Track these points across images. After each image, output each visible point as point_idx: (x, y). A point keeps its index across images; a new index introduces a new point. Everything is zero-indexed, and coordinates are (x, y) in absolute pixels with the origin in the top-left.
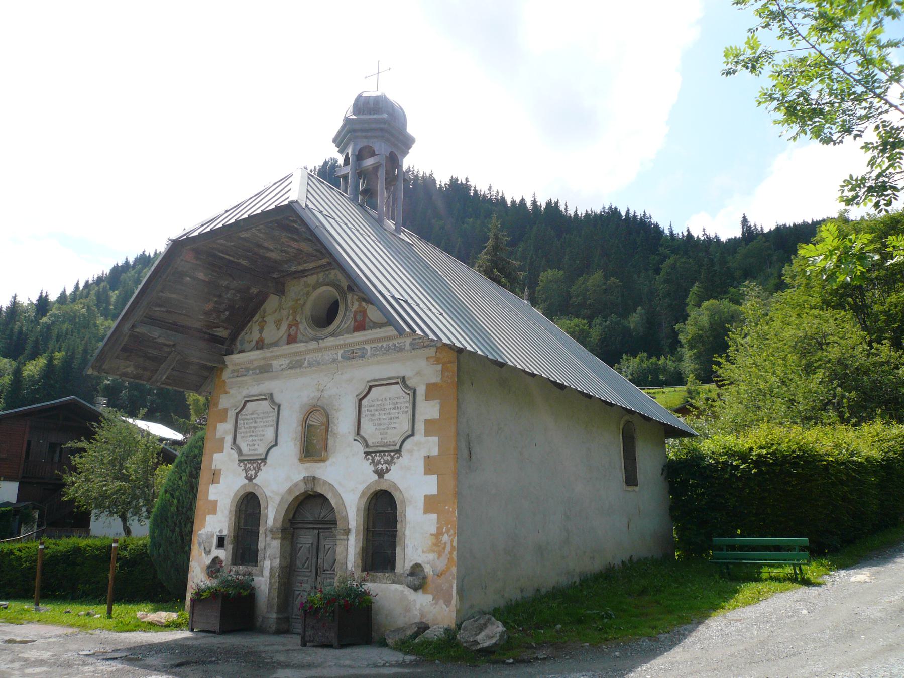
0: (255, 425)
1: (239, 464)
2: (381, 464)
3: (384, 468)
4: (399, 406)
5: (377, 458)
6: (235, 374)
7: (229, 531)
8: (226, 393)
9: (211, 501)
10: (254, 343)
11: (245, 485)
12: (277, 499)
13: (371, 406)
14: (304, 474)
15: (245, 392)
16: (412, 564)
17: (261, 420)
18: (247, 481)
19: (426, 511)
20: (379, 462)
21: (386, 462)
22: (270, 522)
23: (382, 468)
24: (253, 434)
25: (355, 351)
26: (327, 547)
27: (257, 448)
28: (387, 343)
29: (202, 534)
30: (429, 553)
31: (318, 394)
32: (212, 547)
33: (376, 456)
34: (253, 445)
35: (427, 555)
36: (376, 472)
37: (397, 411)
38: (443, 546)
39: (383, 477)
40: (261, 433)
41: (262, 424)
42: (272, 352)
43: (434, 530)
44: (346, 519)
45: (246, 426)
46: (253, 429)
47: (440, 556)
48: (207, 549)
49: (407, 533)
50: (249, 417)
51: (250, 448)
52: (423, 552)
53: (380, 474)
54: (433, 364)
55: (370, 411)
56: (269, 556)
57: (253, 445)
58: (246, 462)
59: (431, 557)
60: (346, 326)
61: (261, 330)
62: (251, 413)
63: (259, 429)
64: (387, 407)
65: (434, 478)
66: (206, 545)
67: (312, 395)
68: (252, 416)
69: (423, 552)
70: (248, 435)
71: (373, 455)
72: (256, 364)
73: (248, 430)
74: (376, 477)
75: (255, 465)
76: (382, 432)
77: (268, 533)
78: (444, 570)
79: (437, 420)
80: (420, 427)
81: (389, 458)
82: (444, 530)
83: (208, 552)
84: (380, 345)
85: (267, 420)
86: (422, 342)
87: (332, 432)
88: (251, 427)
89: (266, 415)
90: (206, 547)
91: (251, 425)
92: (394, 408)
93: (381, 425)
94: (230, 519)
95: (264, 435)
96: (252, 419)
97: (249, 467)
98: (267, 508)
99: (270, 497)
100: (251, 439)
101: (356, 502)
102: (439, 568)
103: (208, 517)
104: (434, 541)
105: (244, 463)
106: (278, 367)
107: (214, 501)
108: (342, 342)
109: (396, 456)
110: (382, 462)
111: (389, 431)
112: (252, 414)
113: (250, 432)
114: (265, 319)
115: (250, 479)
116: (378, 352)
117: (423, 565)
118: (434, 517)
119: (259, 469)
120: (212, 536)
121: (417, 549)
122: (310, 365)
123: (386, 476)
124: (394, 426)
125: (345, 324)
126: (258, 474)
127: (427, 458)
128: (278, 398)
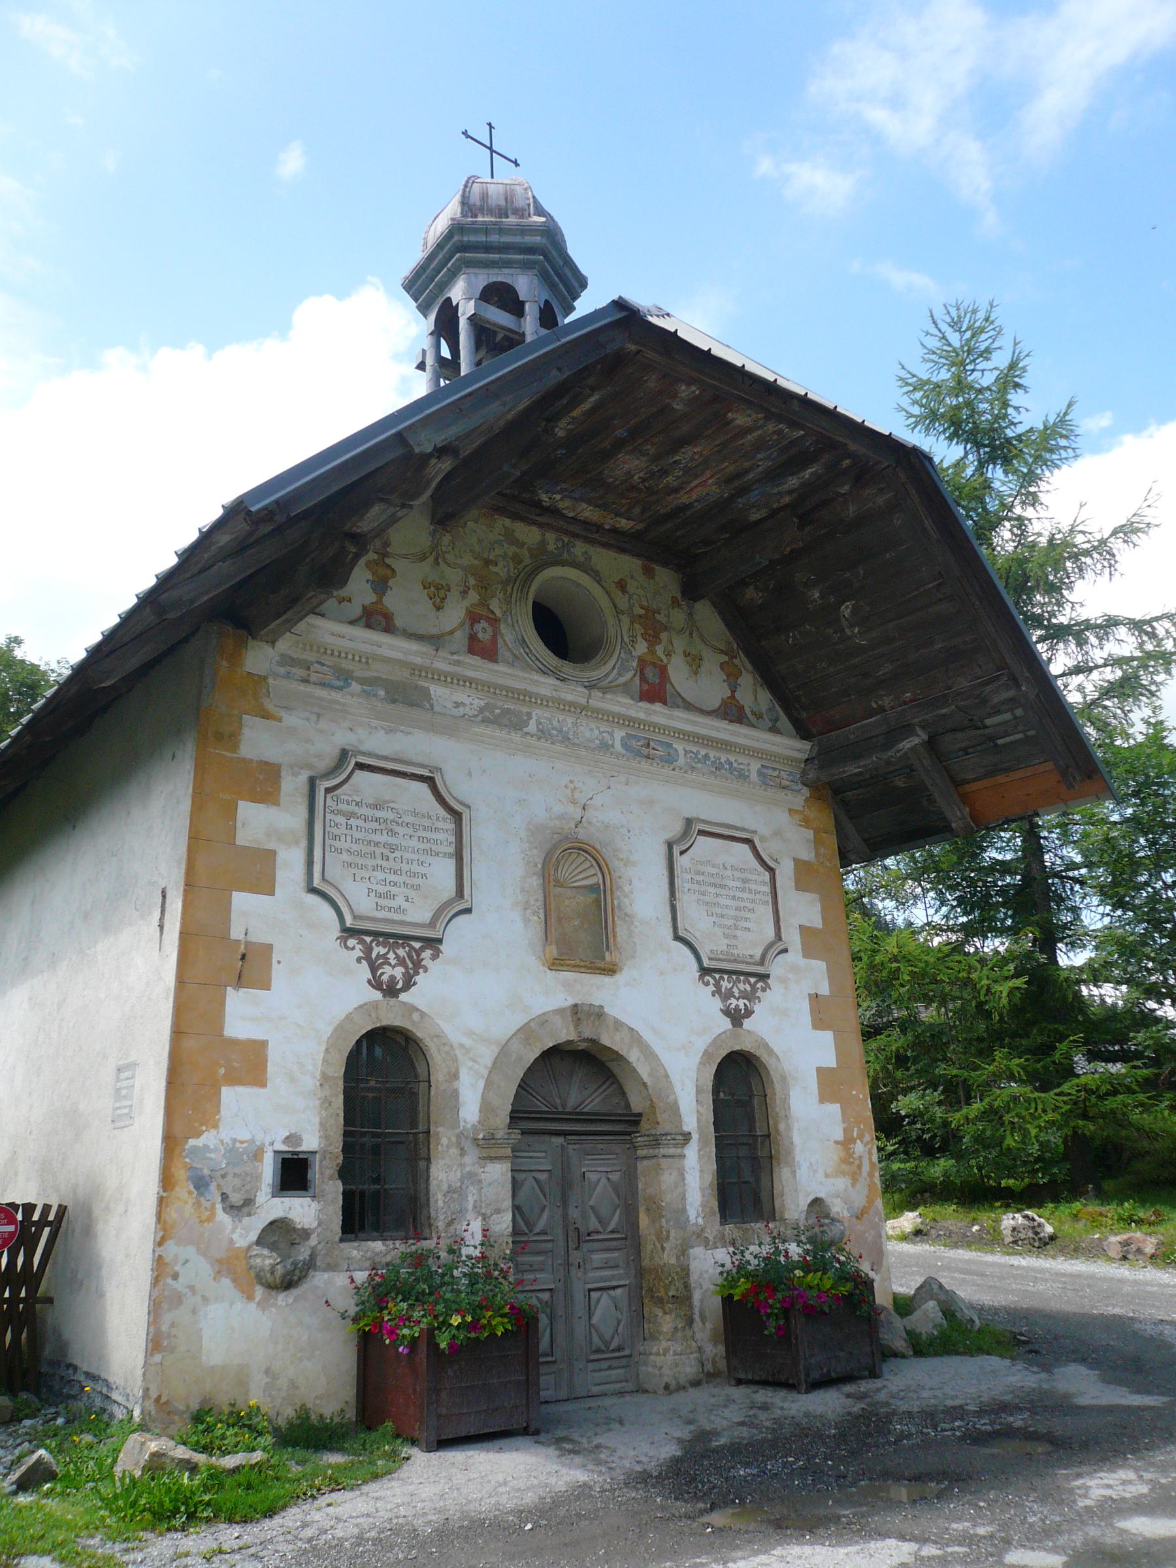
0: (391, 840)
1: (343, 940)
2: (735, 997)
3: (742, 1007)
4: (753, 887)
5: (725, 984)
6: (299, 672)
7: (326, 1137)
8: (267, 716)
9: (234, 1042)
10: (357, 611)
11: (375, 1005)
12: (487, 1055)
13: (698, 873)
14: (562, 1000)
15: (342, 738)
16: (809, 1200)
17: (410, 831)
18: (377, 995)
19: (823, 1099)
20: (729, 995)
21: (744, 995)
22: (470, 1111)
23: (737, 1006)
24: (385, 864)
25: (652, 744)
26: (593, 1177)
27: (405, 905)
28: (717, 754)
29: (206, 1146)
30: (836, 1176)
31: (576, 812)
32: (258, 1189)
33: (722, 978)
34: (387, 896)
35: (833, 1180)
36: (727, 1012)
37: (751, 896)
38: (857, 1163)
39: (741, 1025)
40: (415, 868)
41: (414, 843)
42: (457, 663)
43: (839, 1135)
44: (675, 1109)
45: (357, 835)
46: (386, 852)
47: (854, 1181)
48: (236, 1198)
49: (797, 1139)
50: (364, 811)
51: (381, 902)
52: (827, 1176)
53: (736, 1017)
54: (801, 825)
55: (698, 883)
56: (475, 1207)
57: (387, 896)
58: (368, 939)
59: (841, 1183)
60: (622, 680)
61: (381, 585)
62: (371, 801)
63: (407, 855)
64: (731, 883)
65: (828, 1036)
66: (229, 1185)
67: (558, 809)
68: (379, 814)
69: (827, 1176)
70: (371, 862)
71: (717, 976)
72: (378, 670)
73: (365, 849)
74: (726, 1024)
75: (401, 952)
76: (727, 931)
77: (468, 1145)
78: (864, 1206)
79: (820, 931)
80: (792, 938)
81: (748, 988)
82: (855, 1135)
83: (241, 1208)
84: (703, 752)
85: (435, 836)
86: (778, 777)
87: (619, 908)
88: (377, 844)
89: (427, 823)
90: (228, 1191)
91: (377, 838)
92: (744, 890)
93: (722, 916)
94: (326, 1102)
95: (424, 876)
96: (378, 820)
97: (384, 956)
98: (455, 1076)
99: (462, 1046)
100: (380, 875)
101: (694, 1075)
102: (857, 1204)
103: (228, 1094)
104: (842, 1154)
105: (362, 942)
106: (450, 705)
107: (254, 1042)
108: (642, 715)
109: (759, 985)
110: (737, 995)
111: (739, 933)
112: (376, 807)
113: (373, 855)
114: (387, 560)
115: (391, 991)
116: (699, 765)
117: (828, 1201)
118: (835, 1109)
119: (418, 965)
120: (258, 1155)
121: (815, 1171)
122: (543, 734)
123: (747, 1024)
124: (747, 925)
125: (620, 675)
126: (417, 978)
127: (815, 998)
128: (457, 786)
